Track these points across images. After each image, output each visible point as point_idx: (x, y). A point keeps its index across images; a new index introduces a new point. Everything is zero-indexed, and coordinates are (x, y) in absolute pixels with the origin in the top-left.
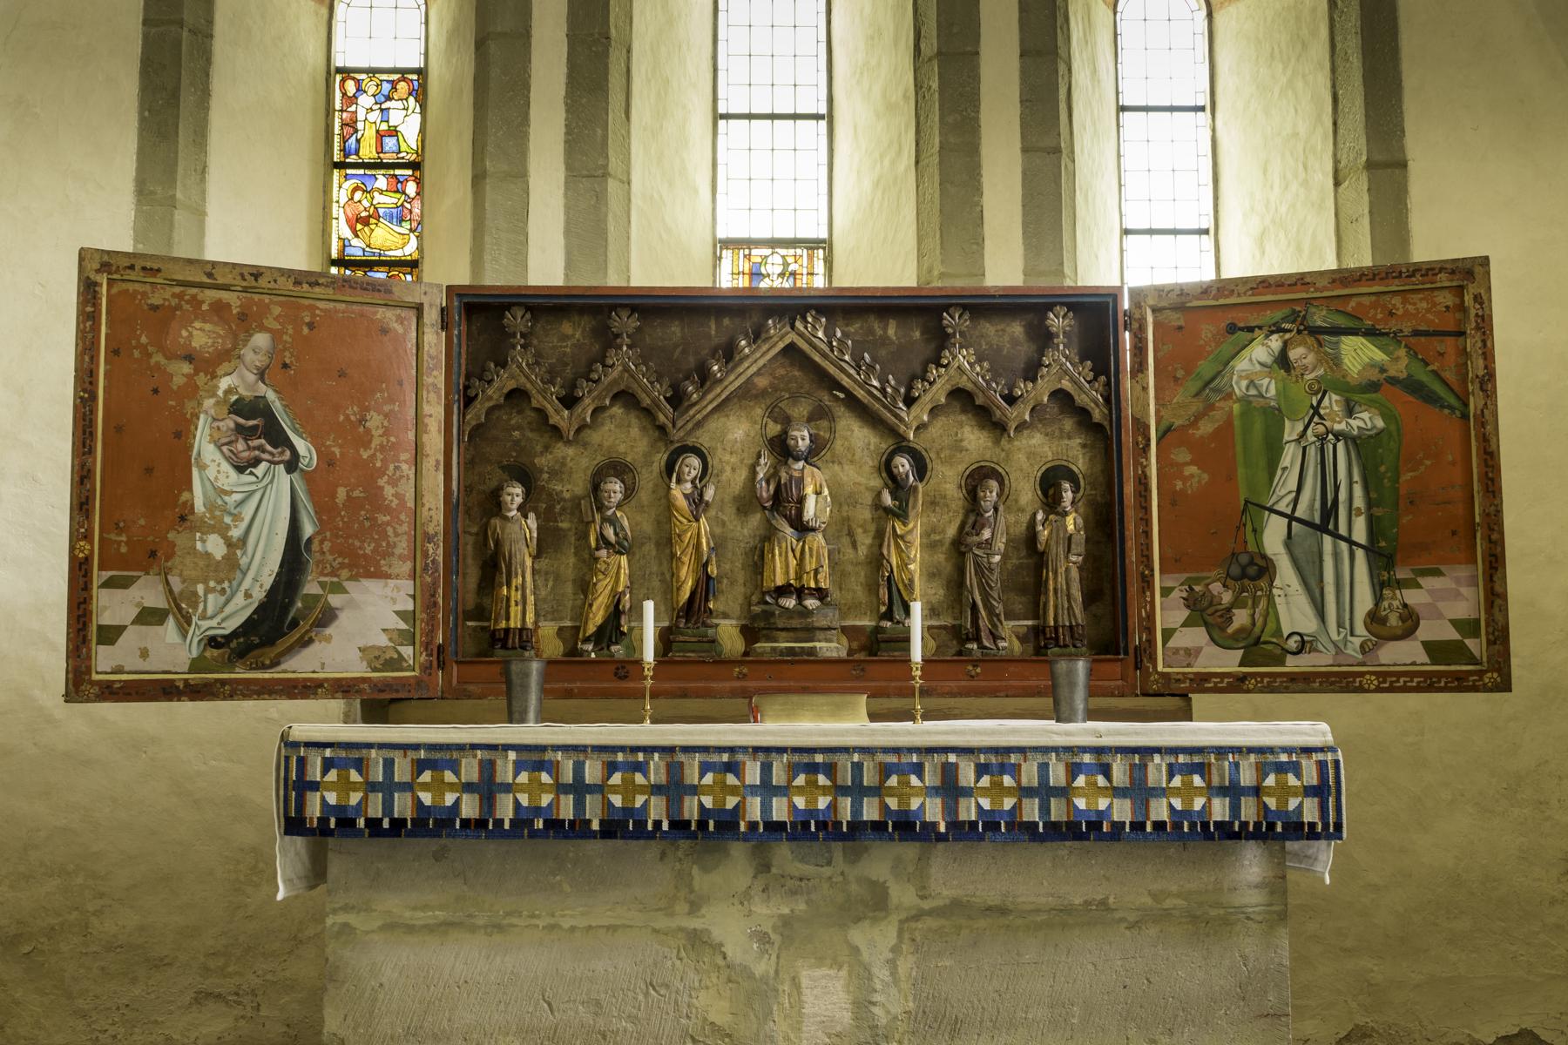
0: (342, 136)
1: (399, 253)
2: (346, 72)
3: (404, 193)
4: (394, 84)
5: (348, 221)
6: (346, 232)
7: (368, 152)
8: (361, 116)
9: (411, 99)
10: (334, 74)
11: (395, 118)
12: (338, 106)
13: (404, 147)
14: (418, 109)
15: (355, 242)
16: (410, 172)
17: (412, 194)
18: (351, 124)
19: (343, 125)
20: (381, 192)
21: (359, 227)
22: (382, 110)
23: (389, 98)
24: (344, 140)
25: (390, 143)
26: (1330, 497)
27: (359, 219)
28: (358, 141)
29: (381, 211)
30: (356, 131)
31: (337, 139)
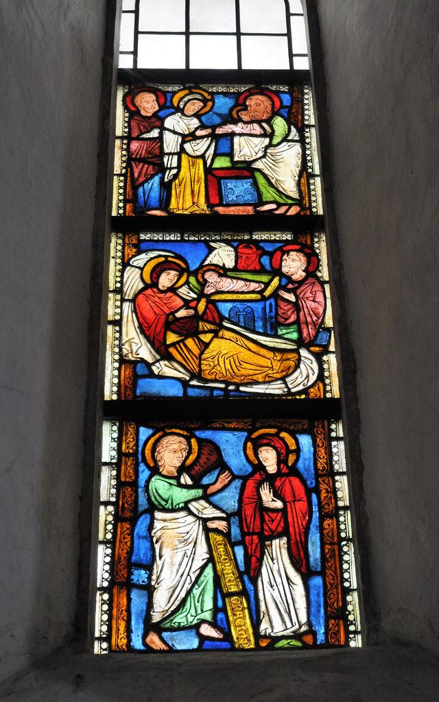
0: (128, 175)
1: (276, 389)
2: (141, 80)
3: (277, 272)
4: (240, 103)
5: (143, 329)
6: (145, 352)
7: (188, 199)
8: (171, 143)
9: (280, 124)
10: (114, 80)
11: (247, 148)
12: (120, 129)
13: (268, 194)
14: (294, 134)
15: (163, 368)
16: (288, 237)
17: (299, 275)
18: (155, 159)
19: (130, 160)
20: (222, 271)
21: (172, 338)
22: (214, 137)
23: (230, 119)
24: (133, 184)
25: (237, 190)
26: (255, 617)
27: (171, 323)
28: (166, 187)
29: (225, 309)
30: (162, 169)
31: (117, 183)
